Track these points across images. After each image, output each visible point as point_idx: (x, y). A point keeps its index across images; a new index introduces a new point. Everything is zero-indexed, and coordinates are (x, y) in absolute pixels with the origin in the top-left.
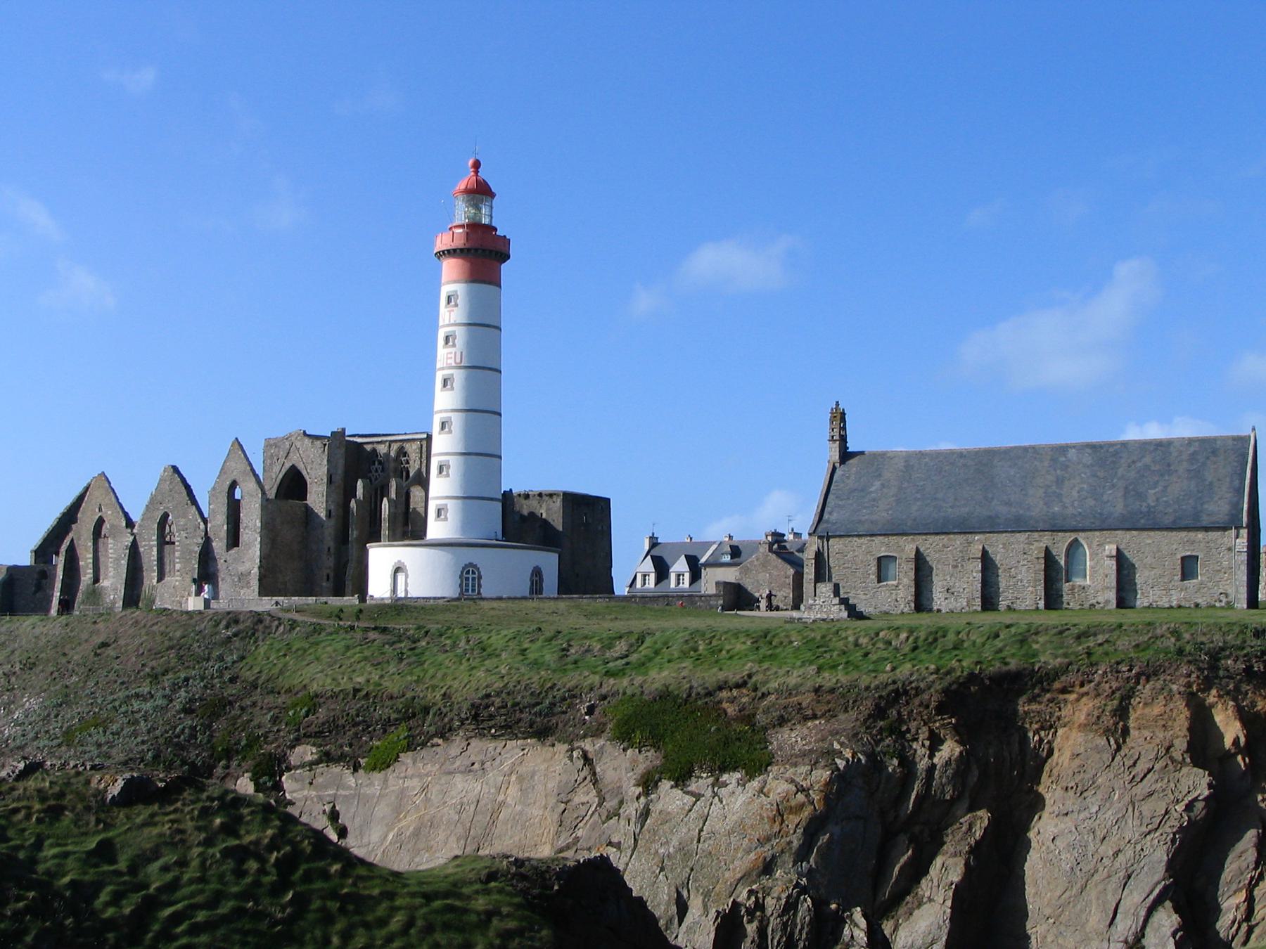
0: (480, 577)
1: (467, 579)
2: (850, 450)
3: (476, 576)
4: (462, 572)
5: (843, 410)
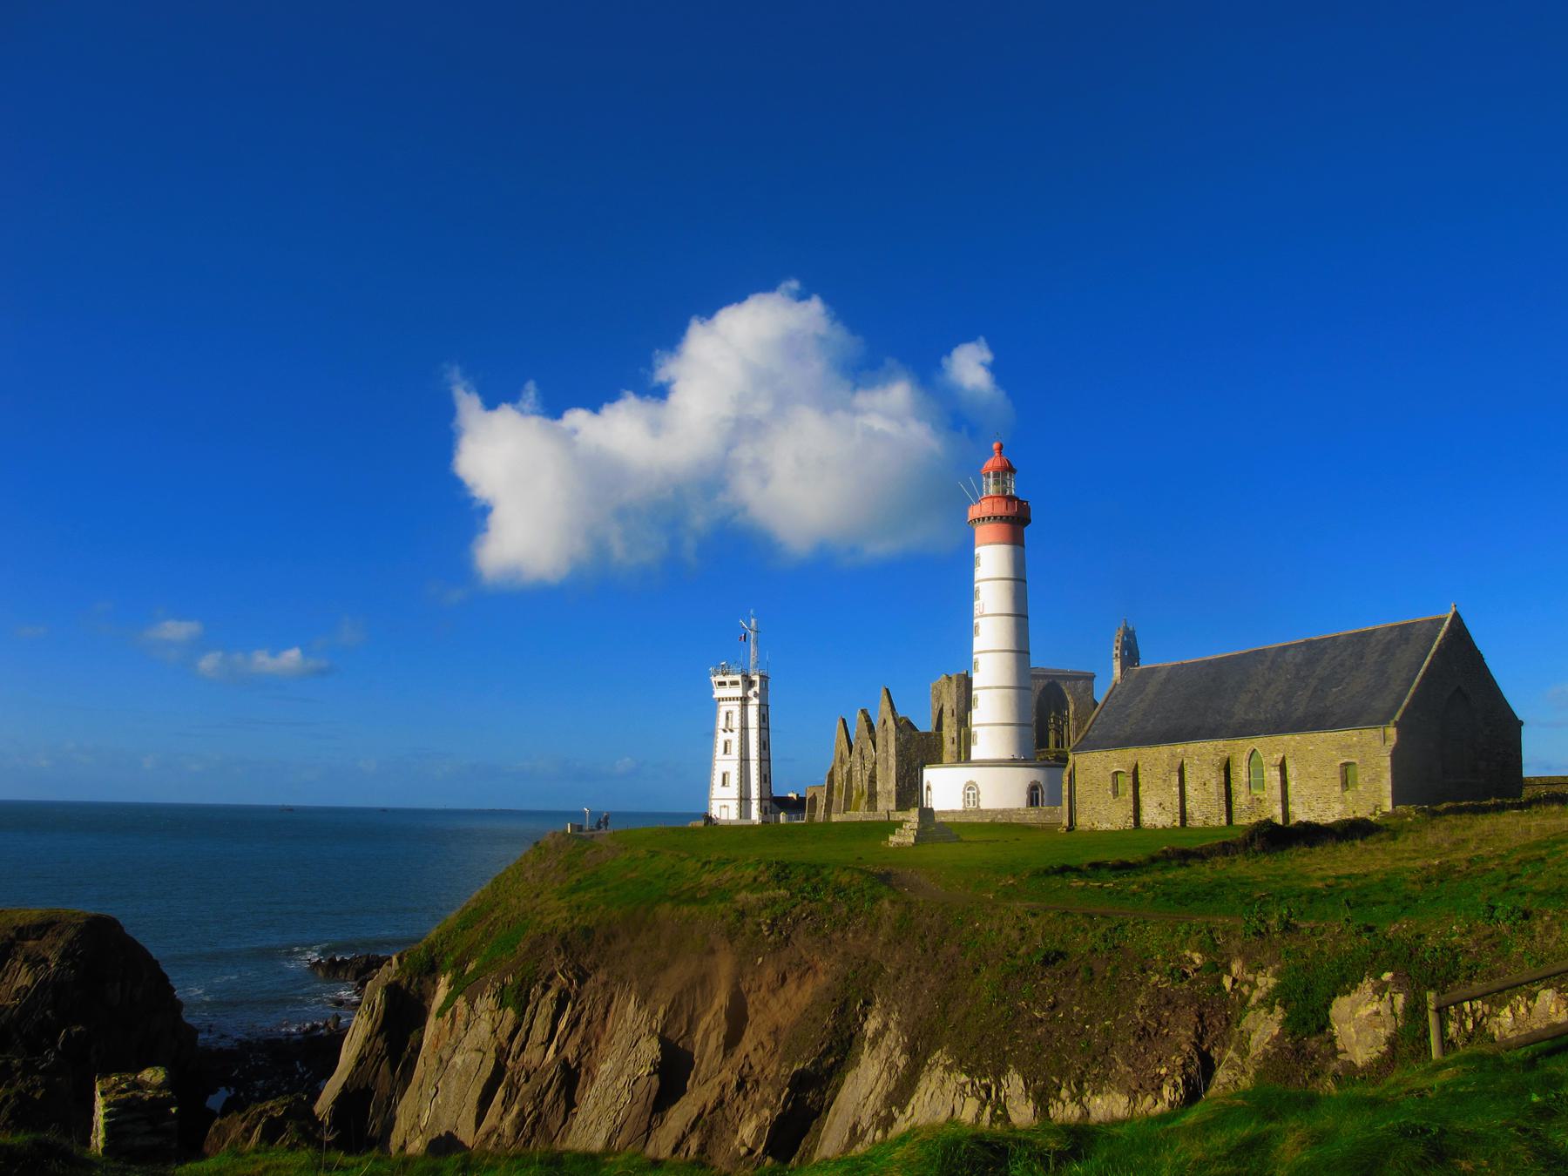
0: (978, 793)
1: (968, 794)
3: (975, 792)
4: (964, 789)
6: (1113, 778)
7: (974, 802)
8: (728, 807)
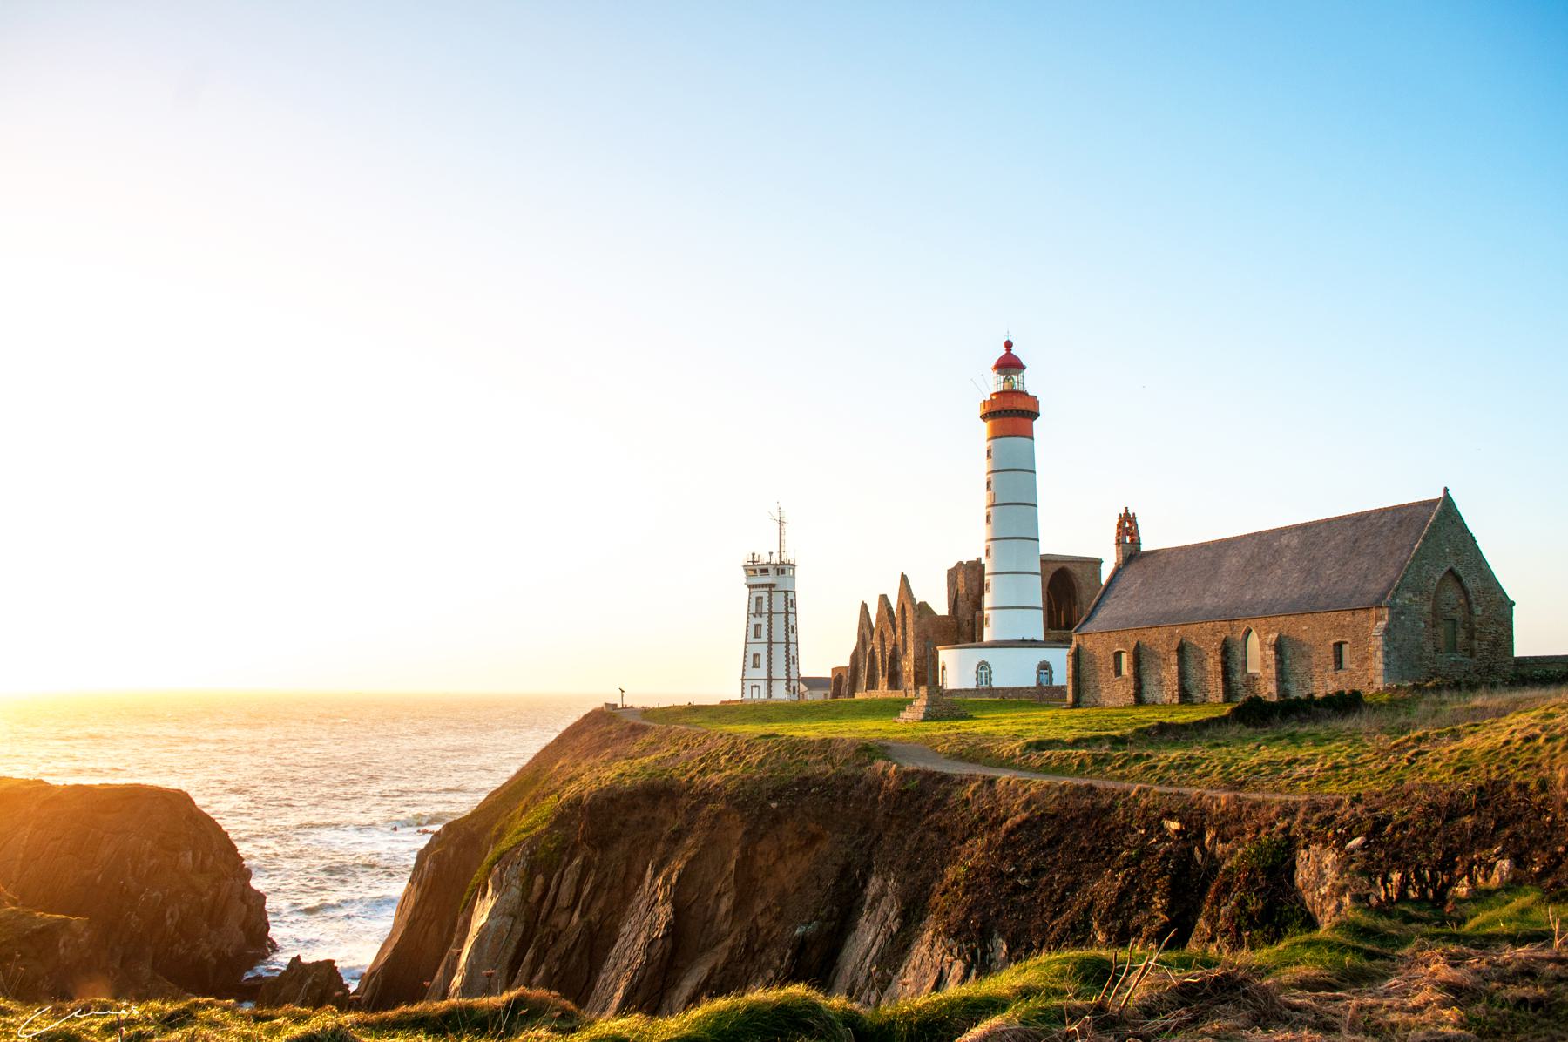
0: (991, 672)
2: (1144, 548)
3: (987, 671)
4: (977, 669)
5: (1134, 514)
6: (1115, 658)
7: (986, 680)
8: (758, 687)
